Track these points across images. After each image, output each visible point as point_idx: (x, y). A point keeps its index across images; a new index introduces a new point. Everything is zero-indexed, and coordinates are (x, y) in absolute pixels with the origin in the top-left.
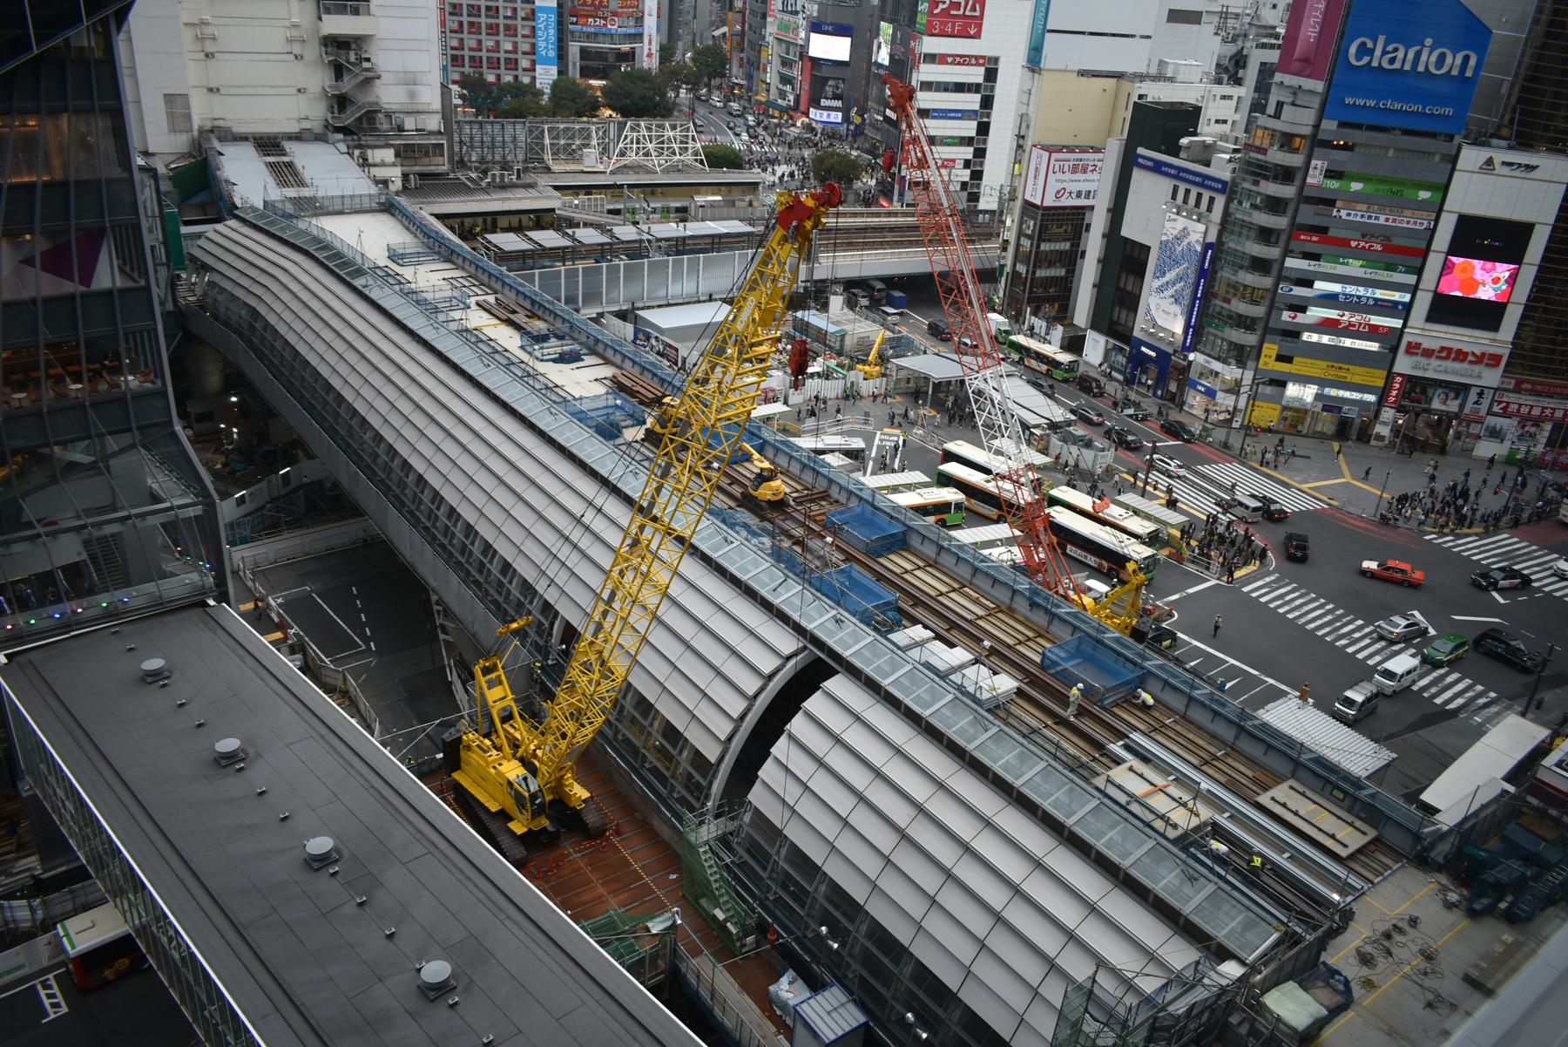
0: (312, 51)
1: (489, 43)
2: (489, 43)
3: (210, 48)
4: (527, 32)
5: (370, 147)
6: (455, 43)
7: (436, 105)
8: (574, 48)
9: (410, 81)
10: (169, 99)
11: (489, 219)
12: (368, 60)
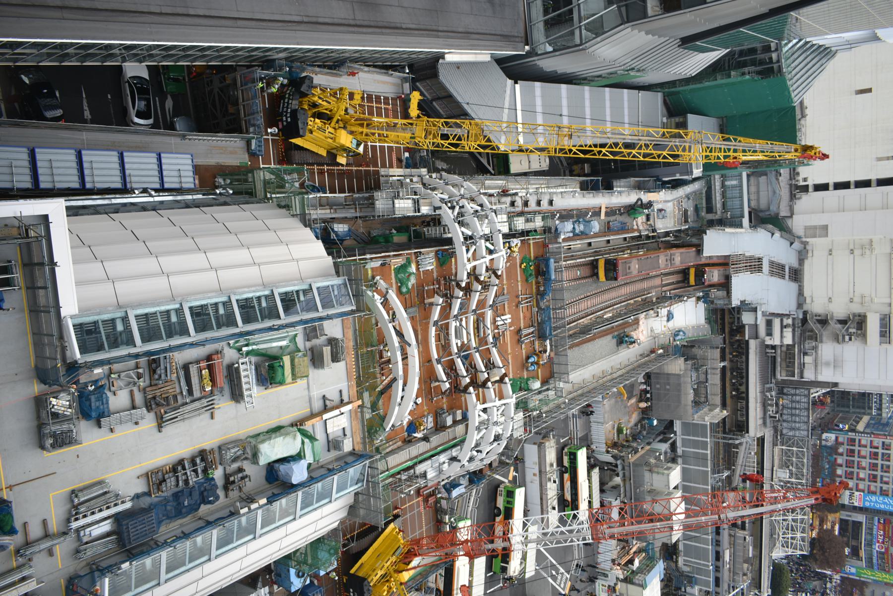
0: (856, 309)
1: (864, 463)
2: (864, 463)
3: (856, 252)
4: (873, 488)
5: (794, 331)
6: (863, 442)
7: (821, 378)
8: (861, 518)
9: (837, 364)
10: (825, 228)
11: (744, 395)
12: (850, 339)
